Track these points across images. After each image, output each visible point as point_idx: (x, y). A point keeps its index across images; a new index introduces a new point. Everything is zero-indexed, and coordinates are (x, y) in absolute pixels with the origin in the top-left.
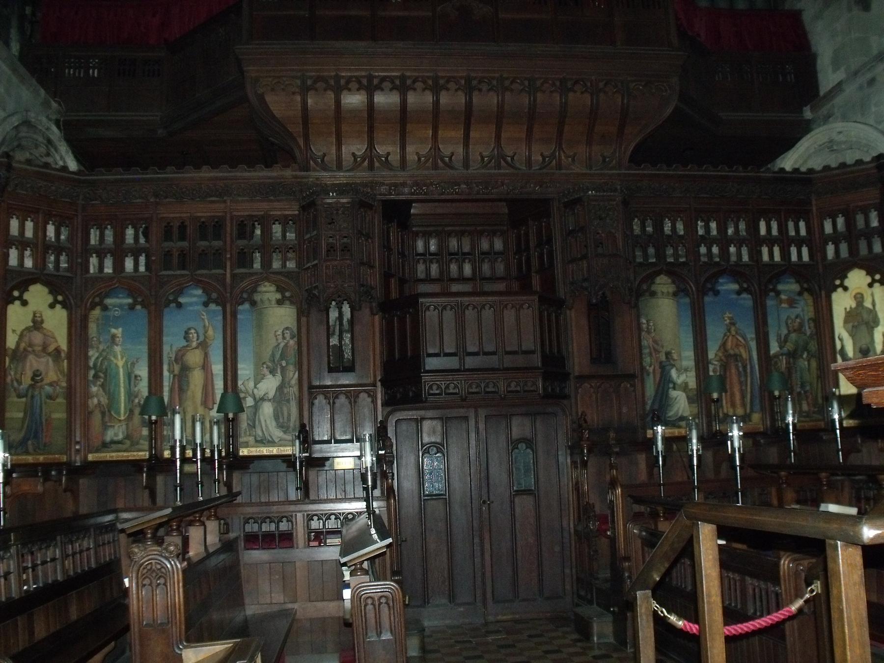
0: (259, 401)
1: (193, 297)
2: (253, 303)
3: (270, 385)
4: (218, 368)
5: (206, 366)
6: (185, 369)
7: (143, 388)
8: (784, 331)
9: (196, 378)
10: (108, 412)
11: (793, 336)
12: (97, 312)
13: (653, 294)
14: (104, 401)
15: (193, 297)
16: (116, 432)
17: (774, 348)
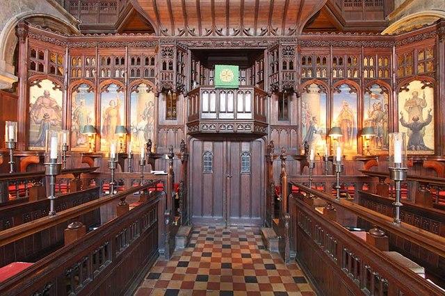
2: (138, 92)
3: (143, 124)
8: (372, 110)
11: (376, 112)
13: (308, 92)
14: (77, 128)
17: (366, 117)
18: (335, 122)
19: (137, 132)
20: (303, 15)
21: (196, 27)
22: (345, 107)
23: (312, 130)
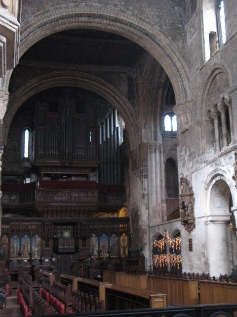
1: (26, 236)
3: (37, 249)
4: (29, 246)
5: (28, 246)
6: (25, 246)
7: (18, 249)
9: (26, 248)
10: (13, 252)
12: (12, 238)
15: (26, 236)
16: (14, 255)
17: (111, 245)
22: (104, 241)
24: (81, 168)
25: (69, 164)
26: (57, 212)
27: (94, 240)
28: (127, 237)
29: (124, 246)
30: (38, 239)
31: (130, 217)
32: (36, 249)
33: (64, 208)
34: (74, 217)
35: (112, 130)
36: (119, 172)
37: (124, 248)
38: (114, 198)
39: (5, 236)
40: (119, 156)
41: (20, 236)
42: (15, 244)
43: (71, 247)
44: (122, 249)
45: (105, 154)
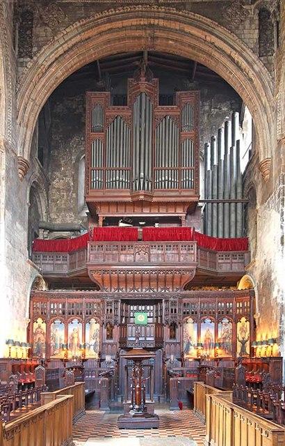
0: (90, 346)
1: (75, 321)
3: (93, 342)
11: (226, 333)
15: (75, 321)
17: (219, 336)
18: (202, 340)
19: (89, 347)
20: (182, 283)
21: (124, 287)
22: (208, 330)
23: (189, 344)
24: (167, 204)
25: (145, 195)
26: (126, 281)
27: (190, 328)
28: (248, 323)
29: (243, 338)
30: (96, 327)
31: (256, 289)
32: (90, 341)
33: (138, 275)
34: (155, 290)
35: (230, 145)
36: (239, 218)
37: (243, 343)
38: (229, 261)
39: (40, 320)
40: (239, 190)
41: (66, 322)
42: (59, 332)
43: (148, 339)
44: (239, 344)
45: (215, 187)
